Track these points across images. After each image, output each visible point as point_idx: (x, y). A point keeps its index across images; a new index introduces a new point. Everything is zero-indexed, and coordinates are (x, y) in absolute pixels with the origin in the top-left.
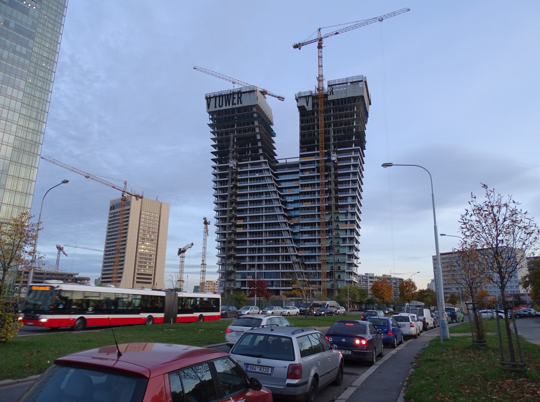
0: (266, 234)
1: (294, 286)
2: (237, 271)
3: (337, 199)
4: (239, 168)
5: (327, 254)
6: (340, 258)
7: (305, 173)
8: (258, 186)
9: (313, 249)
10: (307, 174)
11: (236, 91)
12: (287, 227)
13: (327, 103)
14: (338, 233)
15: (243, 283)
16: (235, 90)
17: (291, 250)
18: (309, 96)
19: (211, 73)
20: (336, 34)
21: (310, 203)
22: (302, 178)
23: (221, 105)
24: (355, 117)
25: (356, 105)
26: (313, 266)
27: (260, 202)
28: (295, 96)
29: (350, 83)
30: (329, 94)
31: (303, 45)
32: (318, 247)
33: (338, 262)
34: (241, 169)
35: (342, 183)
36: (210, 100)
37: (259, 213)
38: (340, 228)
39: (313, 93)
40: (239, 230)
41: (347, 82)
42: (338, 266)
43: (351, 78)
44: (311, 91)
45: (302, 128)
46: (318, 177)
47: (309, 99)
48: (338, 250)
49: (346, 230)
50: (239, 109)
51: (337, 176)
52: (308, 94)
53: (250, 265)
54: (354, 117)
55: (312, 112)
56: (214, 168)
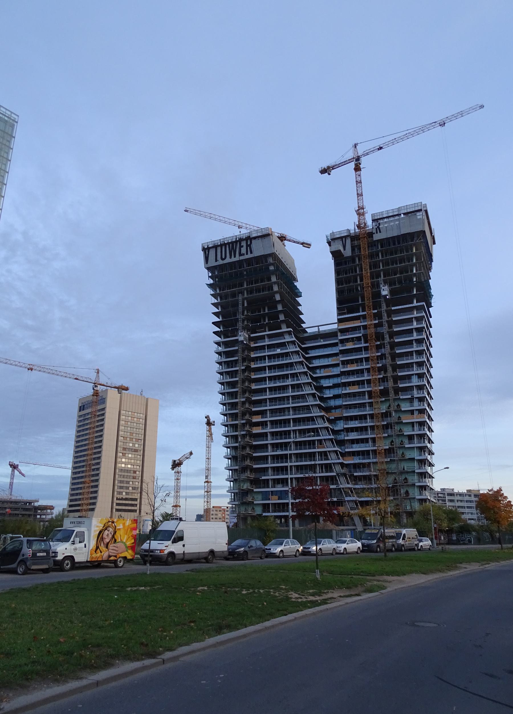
0: (296, 434)
1: (342, 509)
2: (255, 490)
3: (396, 379)
4: (253, 342)
5: (386, 460)
6: (406, 466)
7: (347, 344)
8: (280, 367)
9: (365, 454)
10: (350, 346)
11: (244, 237)
12: (325, 422)
13: (372, 244)
14: (400, 429)
15: (266, 507)
16: (242, 236)
17: (333, 455)
18: (345, 237)
19: (209, 215)
20: (379, 149)
21: (357, 387)
22: (343, 352)
23: (223, 257)
24: (414, 261)
25: (414, 245)
26: (367, 479)
27: (284, 388)
28: (326, 239)
29: (404, 214)
30: (374, 231)
31: (333, 169)
32: (372, 450)
33: (403, 472)
34: (255, 343)
35: (401, 355)
36: (209, 252)
37: (284, 404)
38: (404, 421)
39: (351, 232)
40: (257, 430)
41: (400, 213)
42: (403, 477)
43: (405, 208)
44: (348, 230)
45: (339, 282)
46: (366, 349)
47: (347, 240)
48: (403, 453)
49: (413, 424)
50: (249, 261)
51: (393, 345)
52: (345, 234)
53: (274, 480)
54: (412, 261)
55: (352, 259)
56: (218, 344)
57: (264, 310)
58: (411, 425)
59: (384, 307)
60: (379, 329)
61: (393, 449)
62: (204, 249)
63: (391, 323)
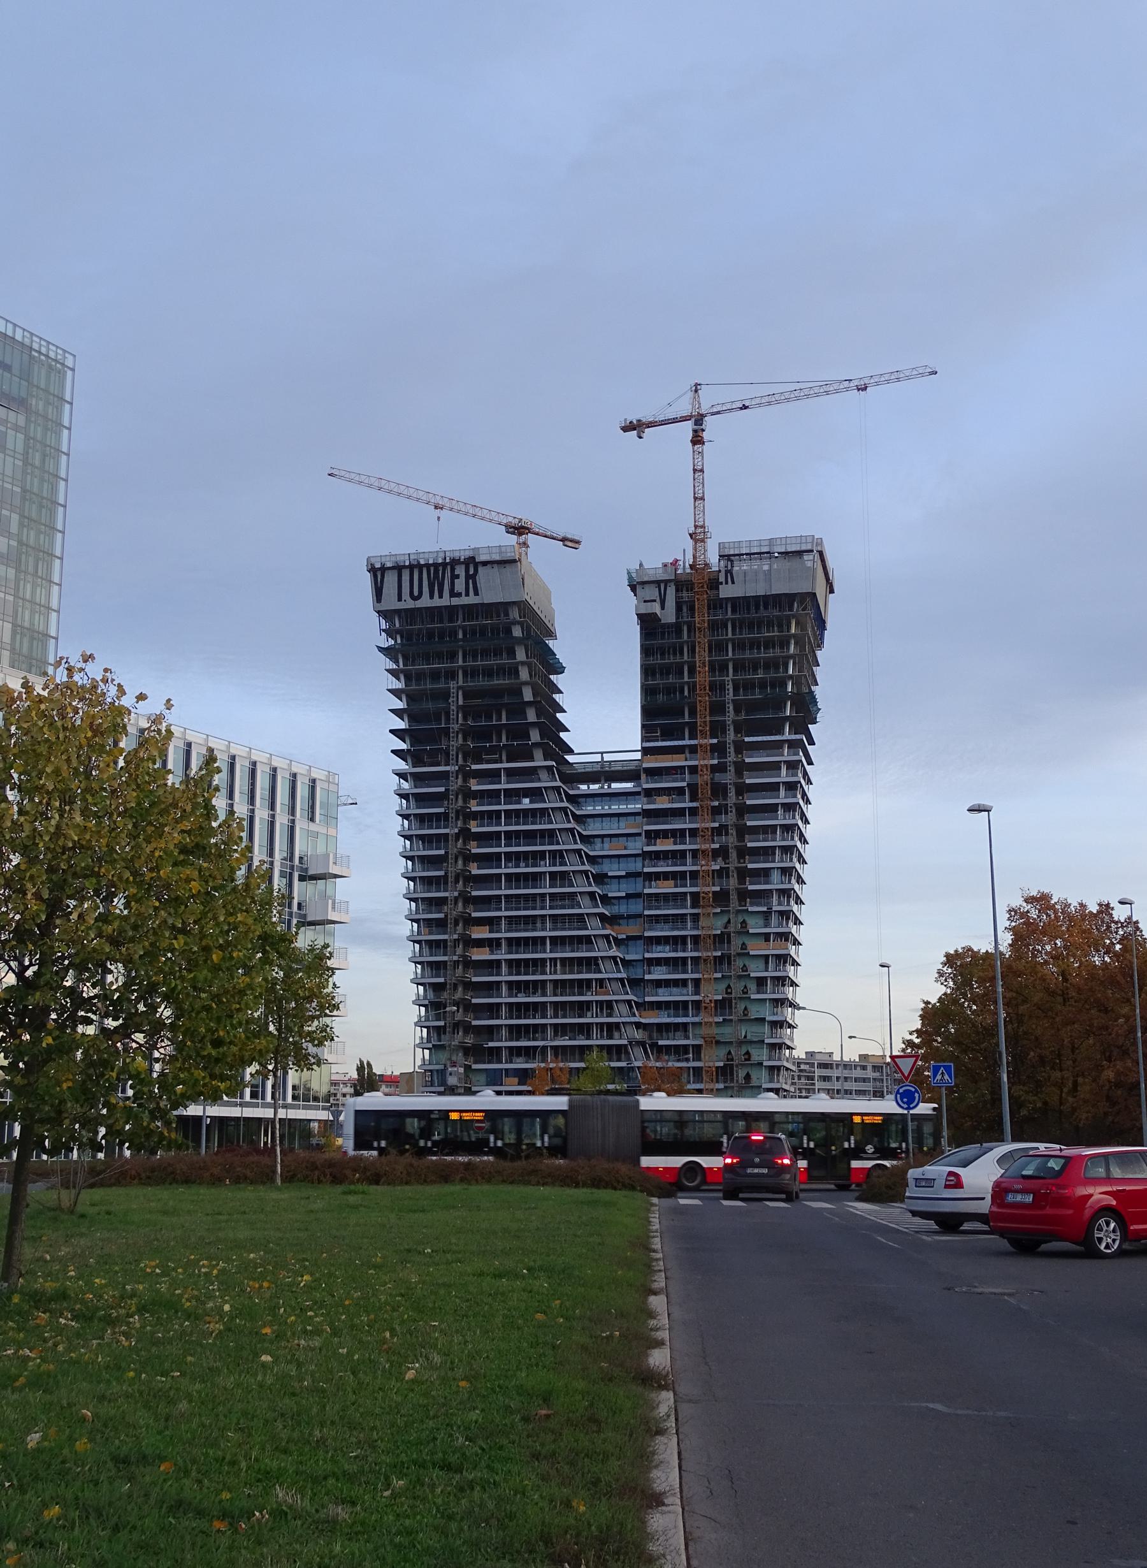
0: (555, 965)
2: (474, 1066)
3: (743, 874)
8: (530, 836)
9: (680, 1007)
10: (662, 803)
12: (610, 948)
13: (717, 604)
14: (744, 966)
21: (672, 882)
23: (416, 593)
25: (794, 616)
26: (680, 1051)
27: (535, 878)
35: (755, 830)
37: (534, 908)
38: (752, 953)
46: (693, 812)
47: (668, 588)
51: (743, 810)
53: (510, 1048)
55: (677, 628)
57: (500, 719)
58: (763, 961)
59: (731, 736)
60: (718, 777)
61: (730, 1000)
62: (372, 570)
63: (741, 768)
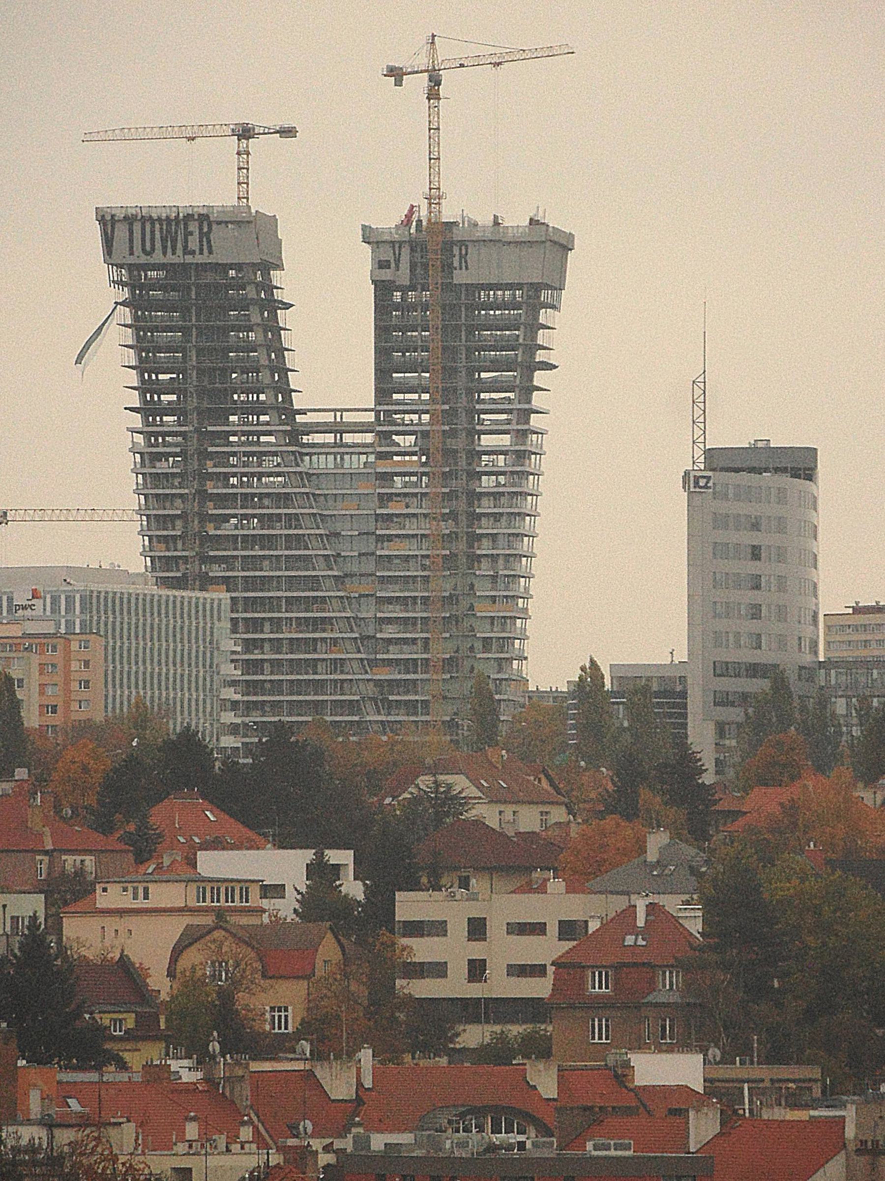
9: (410, 665)
23: (148, 248)
26: (411, 707)
50: (202, 268)
